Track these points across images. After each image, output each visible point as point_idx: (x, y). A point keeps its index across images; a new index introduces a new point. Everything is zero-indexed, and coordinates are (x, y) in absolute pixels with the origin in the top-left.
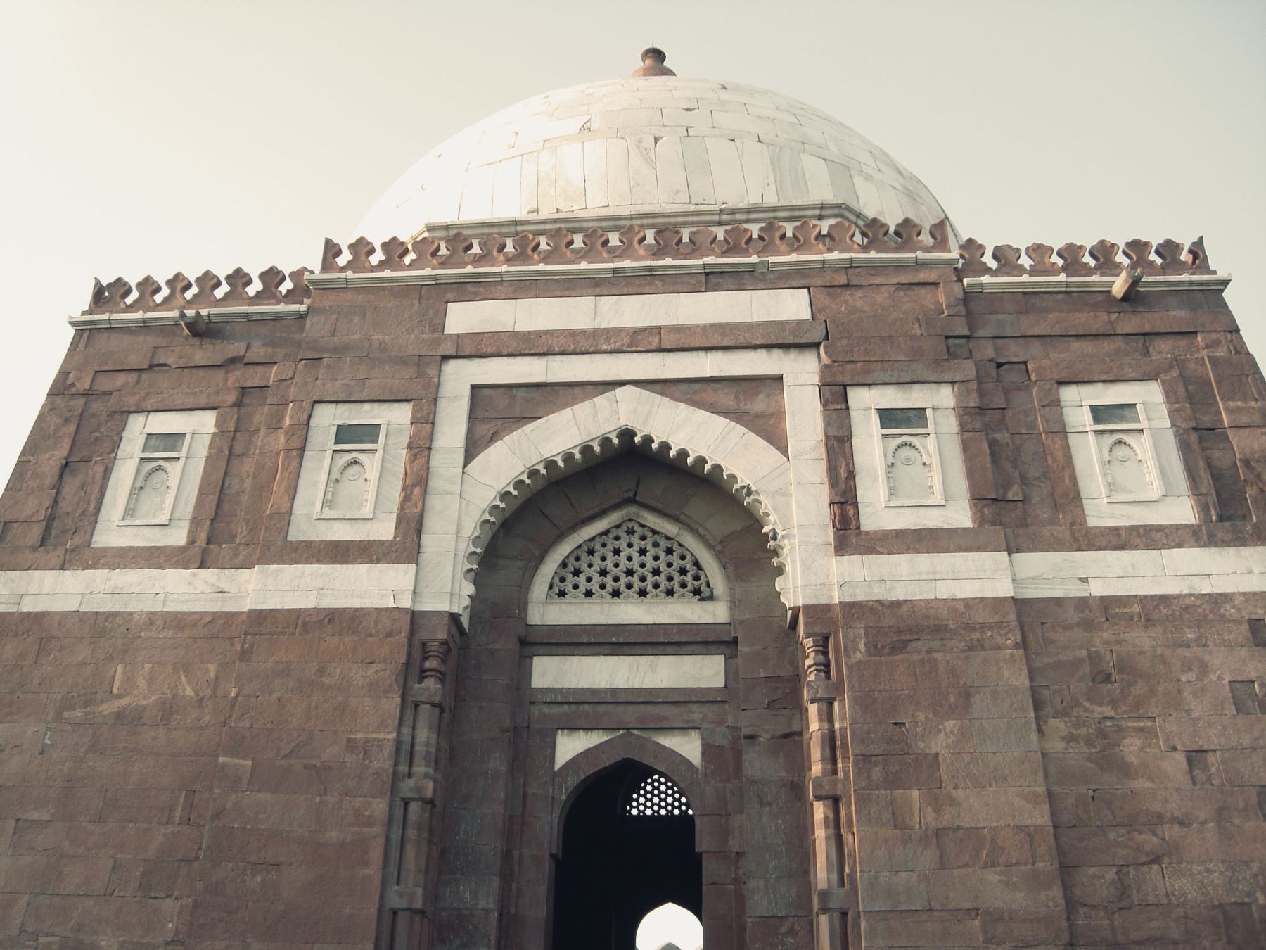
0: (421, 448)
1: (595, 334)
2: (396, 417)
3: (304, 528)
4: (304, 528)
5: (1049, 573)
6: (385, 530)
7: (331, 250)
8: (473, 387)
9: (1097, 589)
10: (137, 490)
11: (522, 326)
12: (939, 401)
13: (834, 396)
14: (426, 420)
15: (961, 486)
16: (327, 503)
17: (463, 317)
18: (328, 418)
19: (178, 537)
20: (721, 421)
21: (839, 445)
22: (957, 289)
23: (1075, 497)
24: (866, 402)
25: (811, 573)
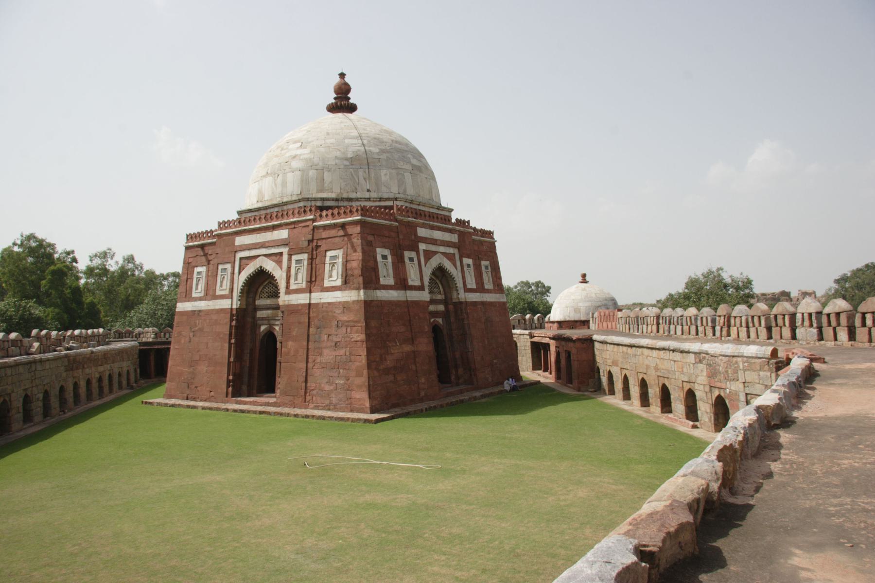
0: (233, 273)
1: (258, 244)
2: (228, 266)
3: (218, 293)
4: (218, 293)
5: (318, 297)
6: (227, 292)
7: (219, 224)
8: (241, 259)
9: (322, 301)
10: (197, 285)
11: (246, 243)
12: (305, 257)
13: (290, 255)
14: (233, 267)
15: (305, 279)
16: (221, 286)
17: (240, 241)
18: (220, 267)
19: (202, 294)
20: (274, 264)
21: (289, 268)
22: (311, 227)
23: (323, 279)
24: (294, 258)
25: (284, 299)
